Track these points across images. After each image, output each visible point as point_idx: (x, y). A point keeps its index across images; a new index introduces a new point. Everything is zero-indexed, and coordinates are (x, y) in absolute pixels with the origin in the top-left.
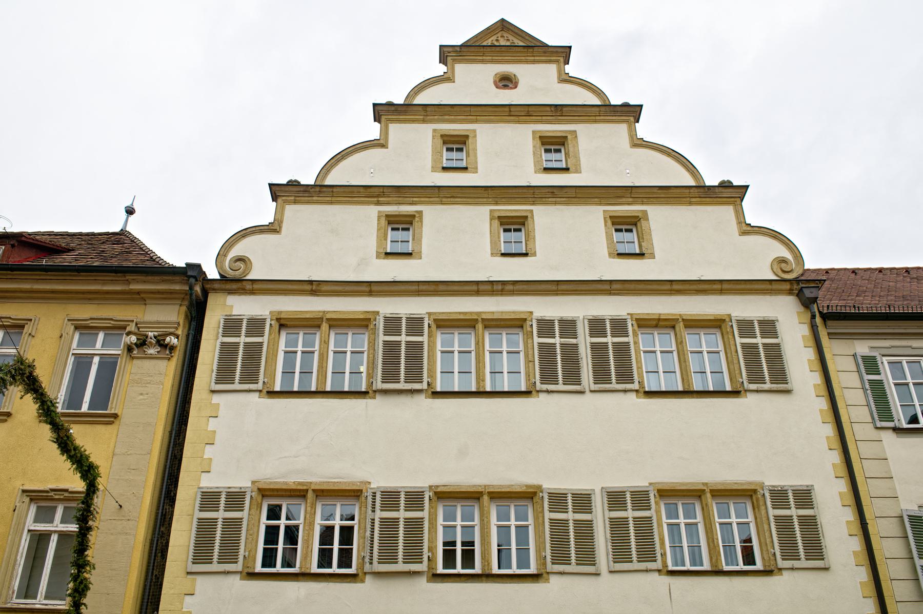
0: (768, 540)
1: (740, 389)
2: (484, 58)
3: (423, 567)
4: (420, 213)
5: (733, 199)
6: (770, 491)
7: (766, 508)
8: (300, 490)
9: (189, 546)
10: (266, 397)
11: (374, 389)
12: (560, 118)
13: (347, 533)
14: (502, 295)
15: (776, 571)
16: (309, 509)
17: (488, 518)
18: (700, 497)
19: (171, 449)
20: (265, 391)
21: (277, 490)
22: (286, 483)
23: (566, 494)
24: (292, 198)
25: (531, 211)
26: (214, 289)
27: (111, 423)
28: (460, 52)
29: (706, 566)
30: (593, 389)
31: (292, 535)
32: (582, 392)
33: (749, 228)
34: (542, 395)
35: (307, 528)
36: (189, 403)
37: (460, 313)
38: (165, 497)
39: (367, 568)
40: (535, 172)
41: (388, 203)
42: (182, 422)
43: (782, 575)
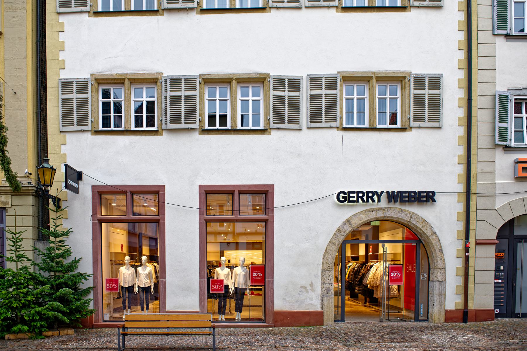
0: (407, 109)
1: (407, 6)
3: (196, 125)
6: (414, 77)
7: (410, 89)
8: (120, 79)
9: (59, 116)
10: (93, 16)
11: (162, 8)
13: (151, 106)
15: (409, 128)
16: (127, 91)
17: (236, 95)
18: (369, 81)
19: (39, 55)
20: (92, 12)
21: (107, 79)
22: (111, 75)
23: (284, 79)
29: (366, 125)
30: (307, 5)
31: (118, 109)
32: (299, 8)
34: (273, 11)
35: (126, 103)
36: (45, 22)
38: (40, 86)
39: (164, 127)
42: (42, 36)
43: (412, 131)
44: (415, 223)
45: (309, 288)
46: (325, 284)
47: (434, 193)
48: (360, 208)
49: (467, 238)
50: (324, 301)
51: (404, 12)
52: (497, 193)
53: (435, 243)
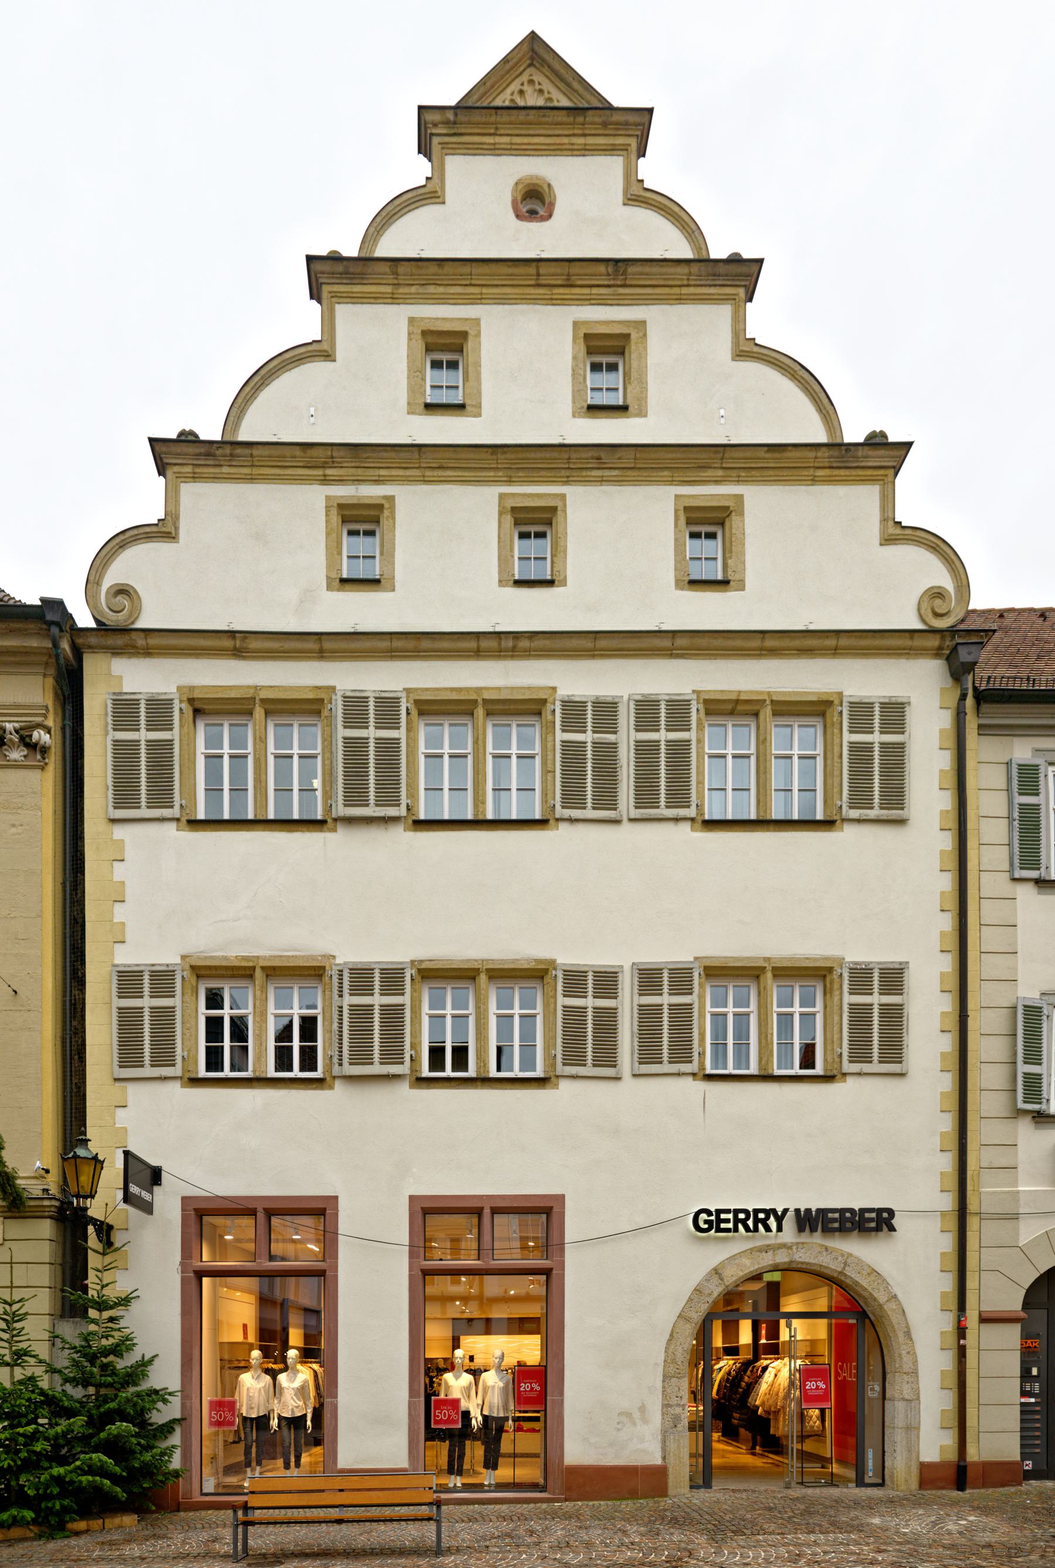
0: (836, 1036)
1: (835, 818)
2: (498, 139)
3: (404, 1069)
4: (391, 499)
5: (882, 472)
6: (850, 969)
7: (841, 994)
8: (245, 968)
9: (111, 1045)
10: (187, 829)
11: (333, 816)
12: (621, 290)
13: (309, 1026)
14: (512, 657)
15: (839, 1076)
16: (258, 993)
17: (486, 1004)
18: (758, 977)
19: (68, 910)
20: (184, 819)
21: (216, 968)
22: (226, 958)
23: (586, 972)
24: (189, 469)
25: (563, 497)
26: (90, 647)
28: (455, 123)
29: (753, 1069)
30: (632, 816)
31: (239, 1031)
32: (617, 822)
33: (898, 531)
34: (563, 827)
35: (258, 1019)
36: (82, 838)
37: (452, 690)
38: (71, 979)
39: (336, 1070)
40: (574, 416)
42: (77, 868)
43: (845, 1081)
44: (853, 1276)
45: (637, 1415)
46: (670, 1406)
47: (891, 1212)
48: (740, 1243)
49: (962, 1306)
50: (668, 1443)
51: (829, 831)
52: (1021, 1211)
53: (895, 1319)
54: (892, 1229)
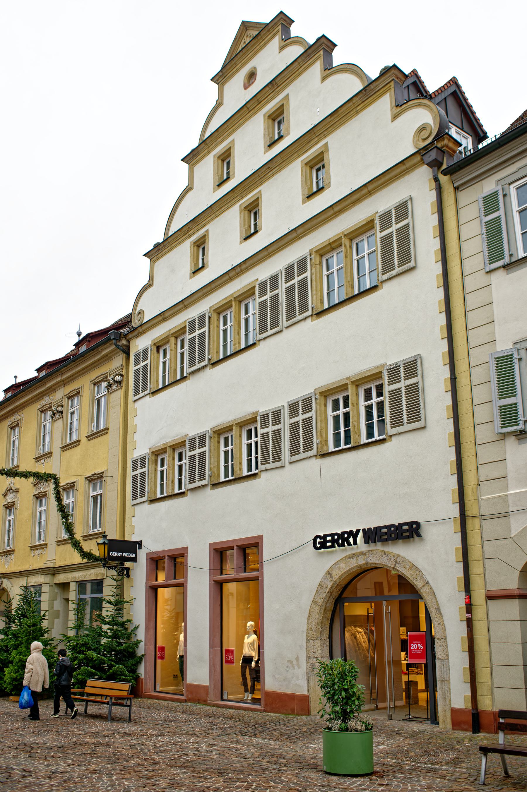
22: (160, 446)
26: (131, 339)
27: (107, 433)
28: (223, 74)
32: (281, 331)
34: (261, 343)
37: (224, 299)
41: (194, 234)
44: (401, 570)
45: (295, 663)
47: (418, 524)
49: (468, 589)
51: (376, 291)
52: (511, 510)
54: (419, 536)
